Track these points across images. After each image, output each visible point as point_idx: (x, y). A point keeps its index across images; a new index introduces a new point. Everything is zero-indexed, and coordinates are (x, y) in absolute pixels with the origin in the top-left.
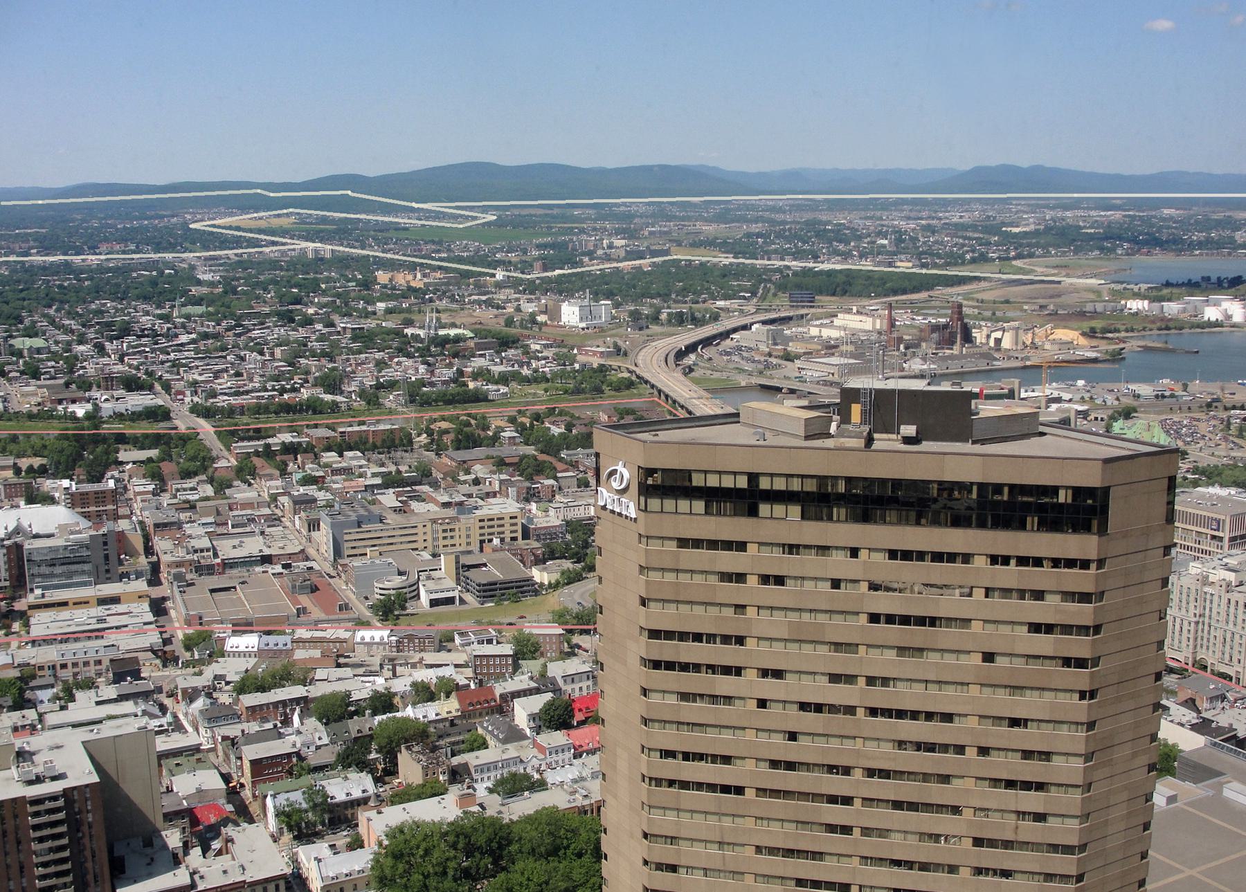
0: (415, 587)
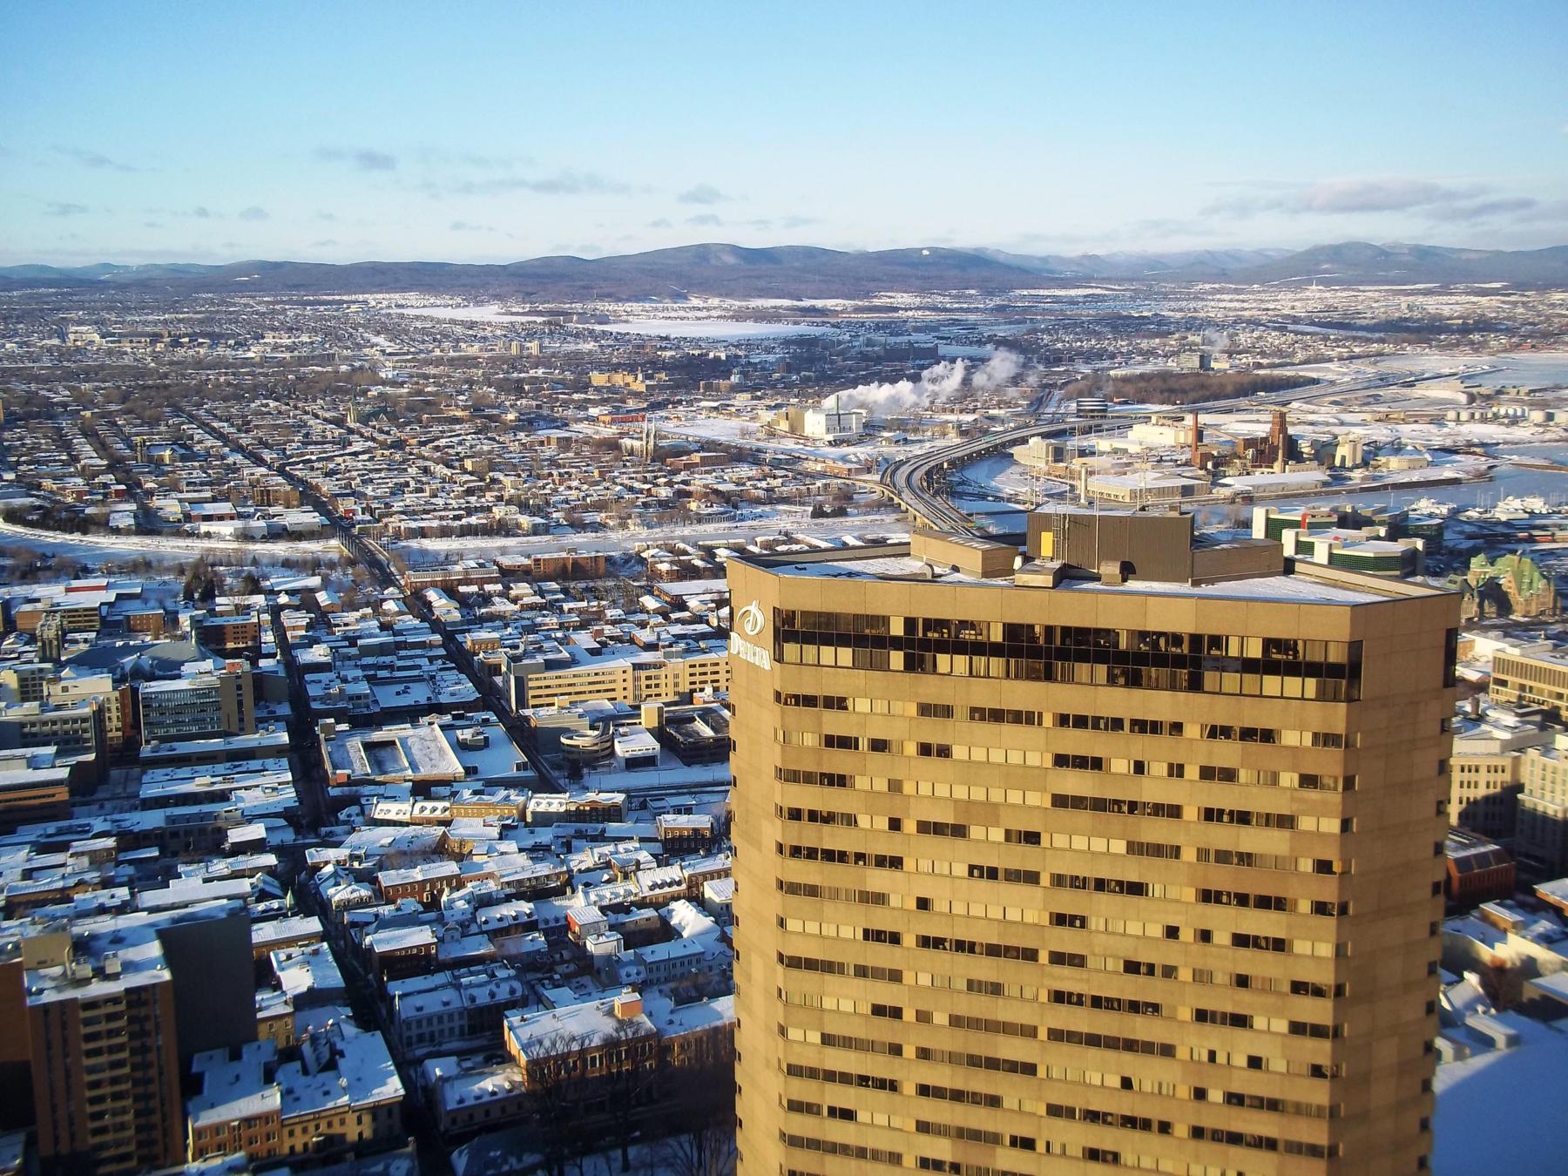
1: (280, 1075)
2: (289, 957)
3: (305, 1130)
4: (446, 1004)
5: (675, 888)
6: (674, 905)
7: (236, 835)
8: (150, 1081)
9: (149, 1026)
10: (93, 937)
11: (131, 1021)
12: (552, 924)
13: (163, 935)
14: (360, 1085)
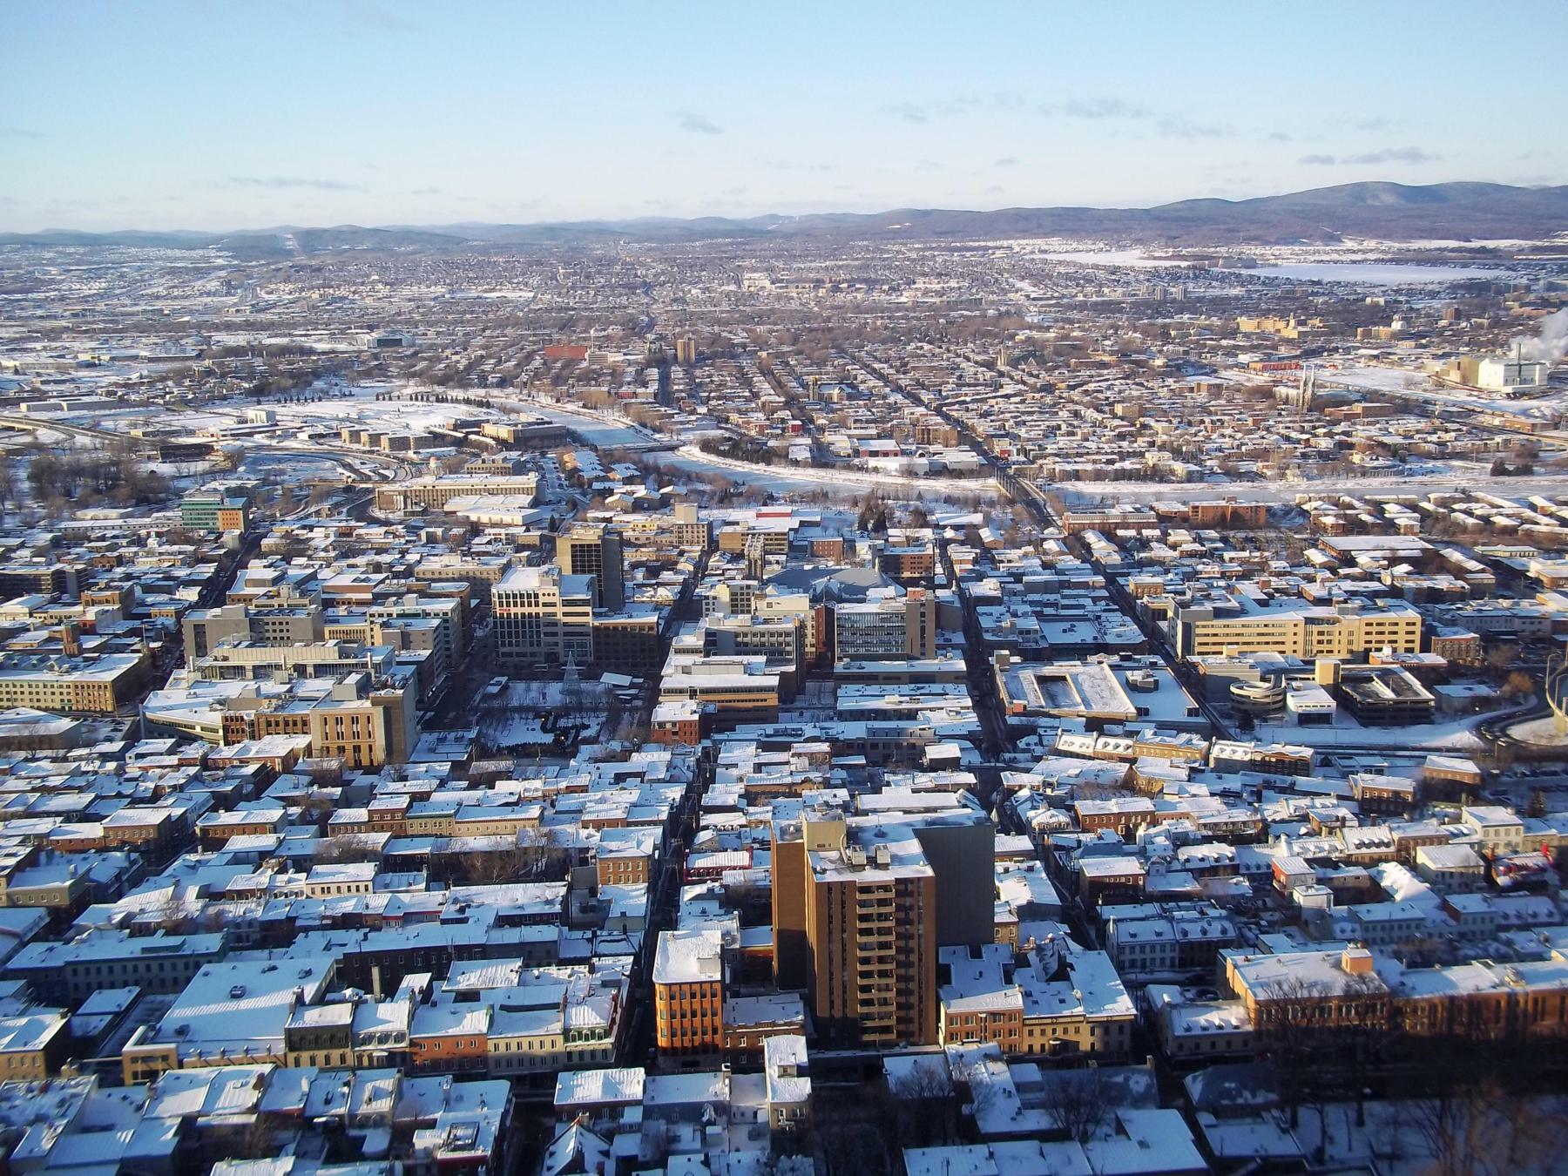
0: (1280, 697)
1: (1015, 977)
2: (1007, 871)
3: (1043, 1032)
4: (1159, 934)
5: (1383, 849)
6: (1383, 866)
7: (934, 752)
8: (911, 965)
9: (913, 915)
10: (860, 829)
11: (899, 908)
12: (1254, 871)
13: (919, 834)
14: (1090, 998)
